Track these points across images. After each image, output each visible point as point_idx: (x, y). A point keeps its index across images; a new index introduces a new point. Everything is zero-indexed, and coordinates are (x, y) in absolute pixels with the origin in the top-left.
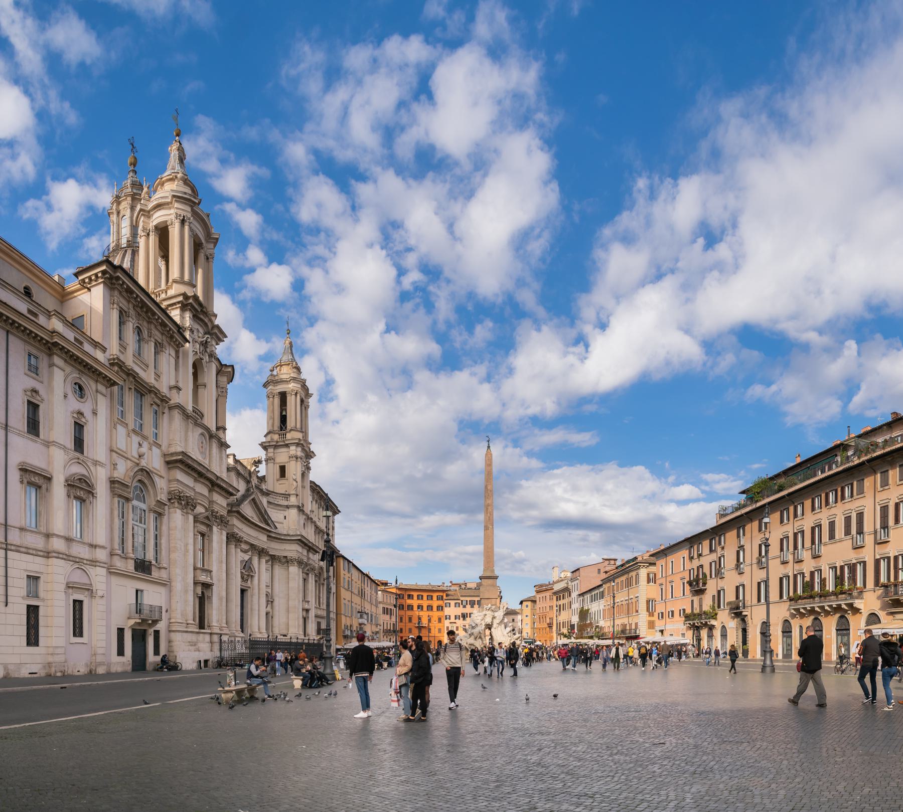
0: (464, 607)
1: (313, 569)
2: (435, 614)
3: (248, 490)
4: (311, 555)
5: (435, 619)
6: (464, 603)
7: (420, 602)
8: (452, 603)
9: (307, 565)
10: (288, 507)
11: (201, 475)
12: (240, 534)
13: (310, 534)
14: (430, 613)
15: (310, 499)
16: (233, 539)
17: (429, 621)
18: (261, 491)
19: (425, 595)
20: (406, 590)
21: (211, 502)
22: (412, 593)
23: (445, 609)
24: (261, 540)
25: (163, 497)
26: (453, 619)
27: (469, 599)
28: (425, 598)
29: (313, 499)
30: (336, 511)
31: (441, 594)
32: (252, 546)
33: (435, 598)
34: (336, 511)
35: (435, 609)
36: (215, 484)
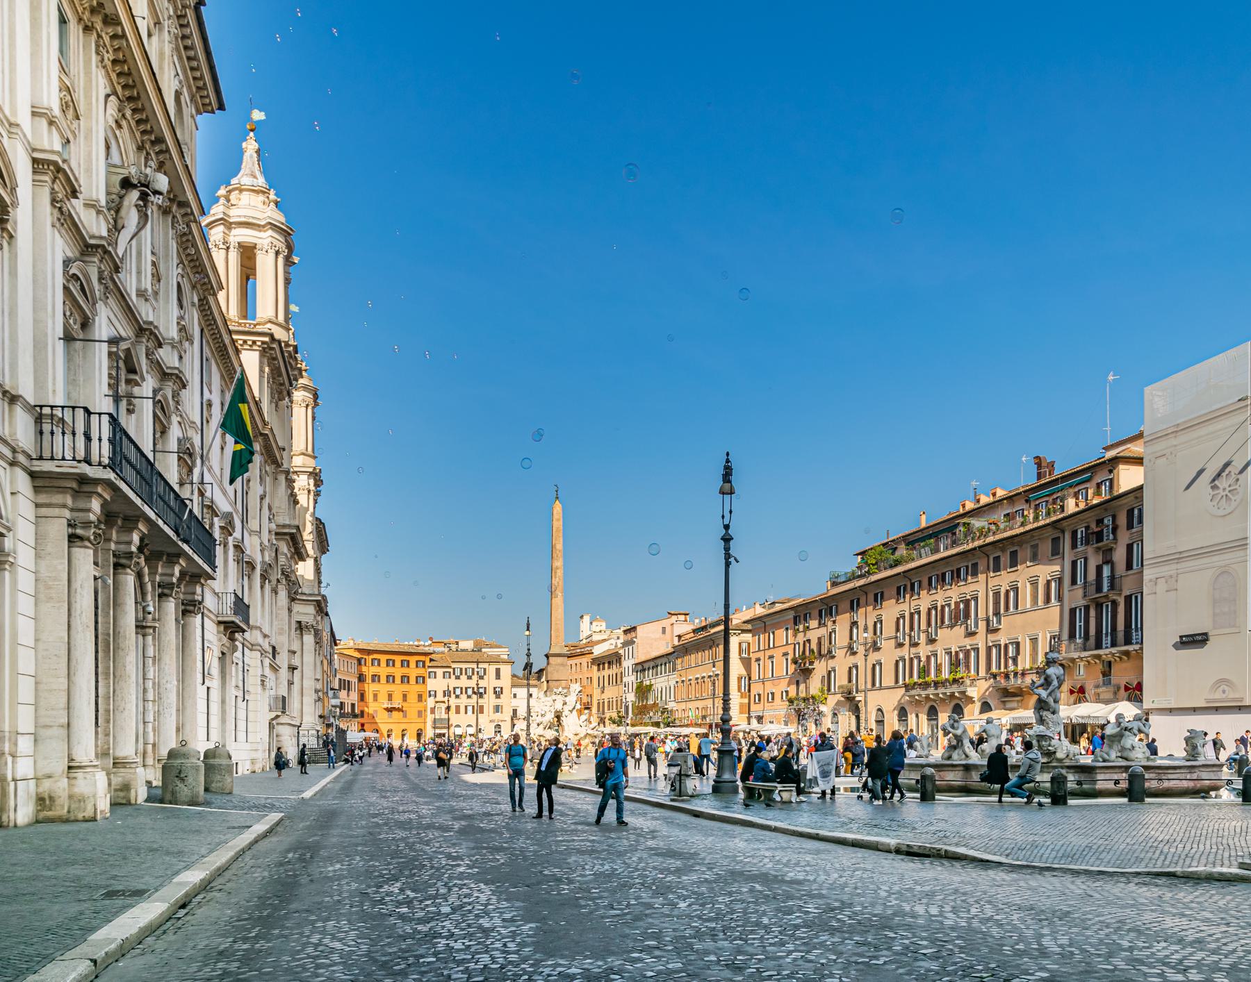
0: (458, 678)
2: (413, 689)
5: (413, 698)
6: (458, 673)
7: (390, 670)
8: (440, 672)
14: (405, 687)
17: (405, 696)
19: (398, 659)
20: (369, 652)
22: (375, 656)
23: (429, 681)
26: (440, 697)
27: (464, 666)
28: (398, 664)
31: (422, 658)
33: (413, 665)
35: (413, 680)
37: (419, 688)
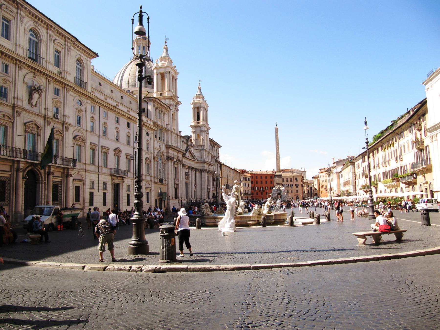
1: (211, 172)
3: (187, 147)
4: (210, 167)
9: (209, 171)
10: (201, 150)
11: (175, 150)
12: (185, 164)
13: (209, 159)
15: (209, 145)
16: (184, 166)
18: (191, 146)
21: (178, 157)
24: (192, 164)
25: (166, 159)
29: (210, 144)
30: (219, 146)
32: (189, 167)
34: (219, 146)
36: (179, 151)
37: (272, 185)
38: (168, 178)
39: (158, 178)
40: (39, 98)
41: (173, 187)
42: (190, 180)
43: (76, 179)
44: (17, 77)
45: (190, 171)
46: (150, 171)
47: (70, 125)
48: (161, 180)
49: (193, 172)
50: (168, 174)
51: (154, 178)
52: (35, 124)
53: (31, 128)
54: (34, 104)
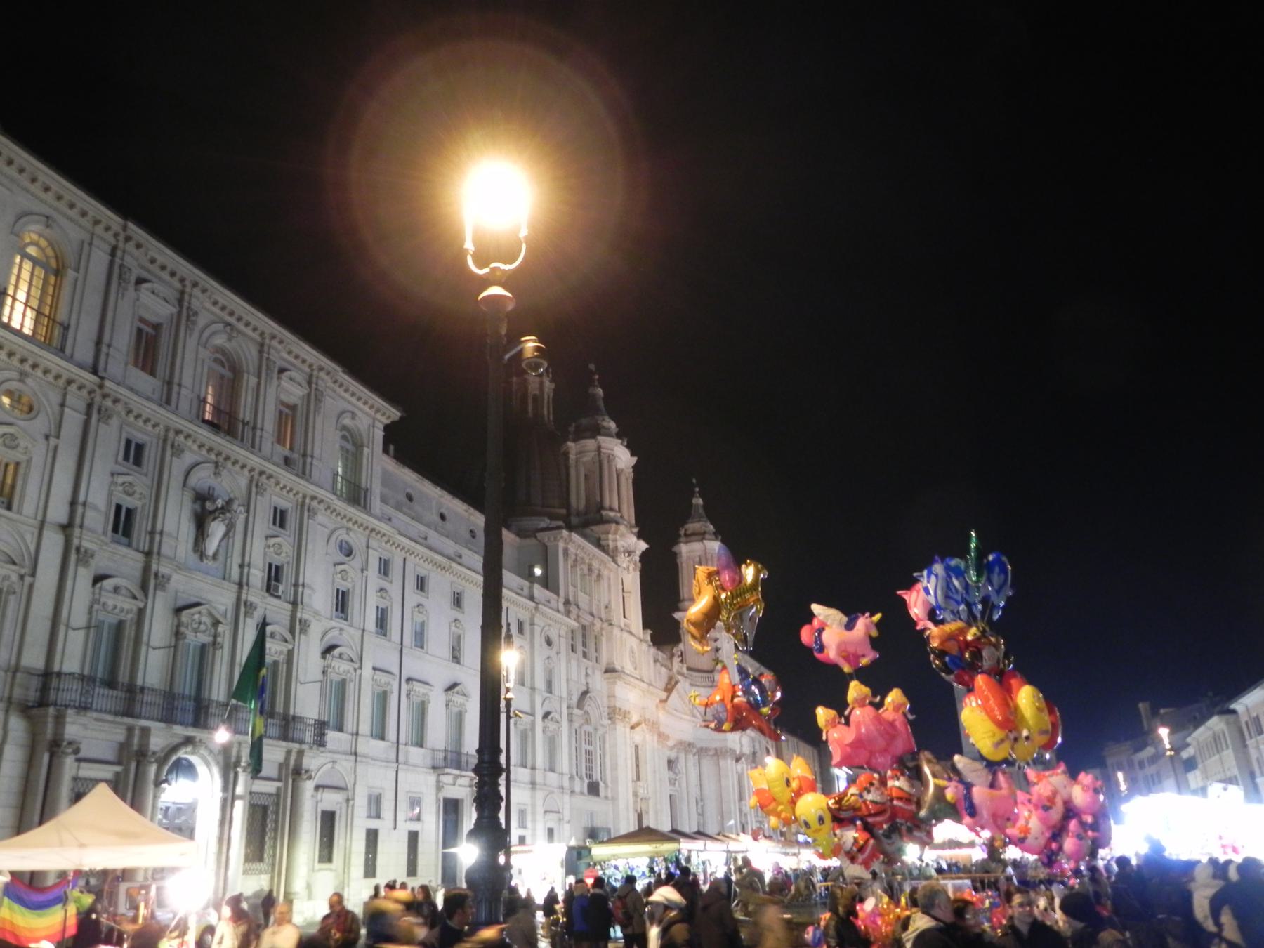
38: (615, 781)
39: (581, 778)
40: (226, 535)
41: (631, 810)
42: (684, 785)
43: (324, 787)
44: (165, 477)
45: (682, 756)
46: (558, 756)
47: (316, 613)
48: (594, 789)
49: (692, 760)
50: (614, 767)
51: (571, 778)
52: (210, 614)
53: (195, 626)
54: (210, 552)
